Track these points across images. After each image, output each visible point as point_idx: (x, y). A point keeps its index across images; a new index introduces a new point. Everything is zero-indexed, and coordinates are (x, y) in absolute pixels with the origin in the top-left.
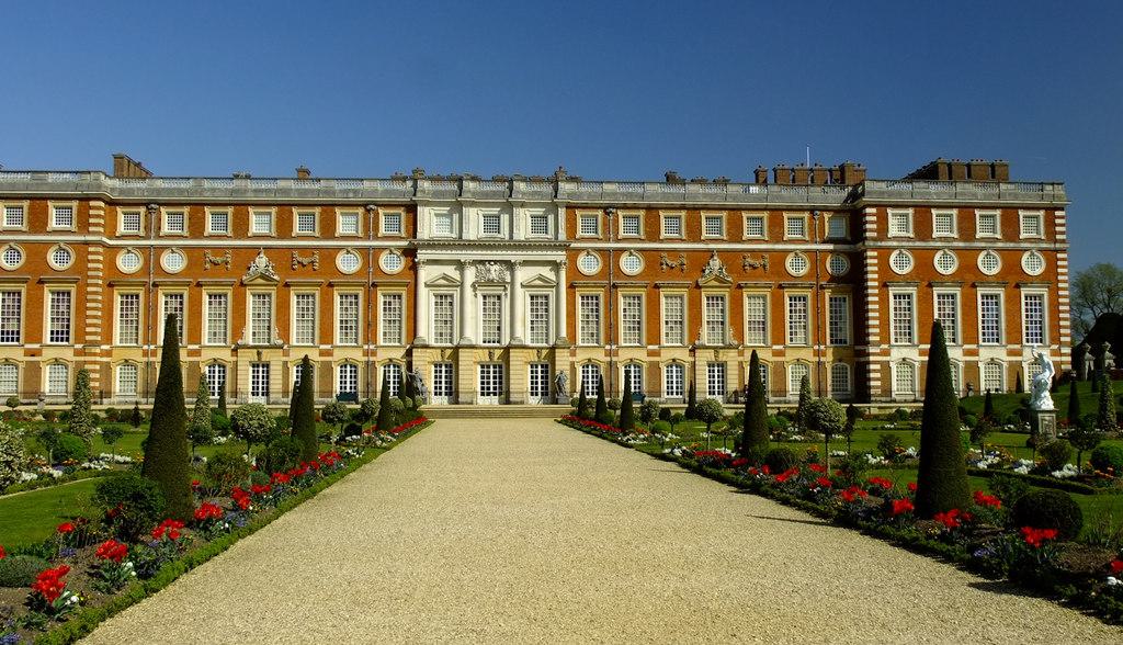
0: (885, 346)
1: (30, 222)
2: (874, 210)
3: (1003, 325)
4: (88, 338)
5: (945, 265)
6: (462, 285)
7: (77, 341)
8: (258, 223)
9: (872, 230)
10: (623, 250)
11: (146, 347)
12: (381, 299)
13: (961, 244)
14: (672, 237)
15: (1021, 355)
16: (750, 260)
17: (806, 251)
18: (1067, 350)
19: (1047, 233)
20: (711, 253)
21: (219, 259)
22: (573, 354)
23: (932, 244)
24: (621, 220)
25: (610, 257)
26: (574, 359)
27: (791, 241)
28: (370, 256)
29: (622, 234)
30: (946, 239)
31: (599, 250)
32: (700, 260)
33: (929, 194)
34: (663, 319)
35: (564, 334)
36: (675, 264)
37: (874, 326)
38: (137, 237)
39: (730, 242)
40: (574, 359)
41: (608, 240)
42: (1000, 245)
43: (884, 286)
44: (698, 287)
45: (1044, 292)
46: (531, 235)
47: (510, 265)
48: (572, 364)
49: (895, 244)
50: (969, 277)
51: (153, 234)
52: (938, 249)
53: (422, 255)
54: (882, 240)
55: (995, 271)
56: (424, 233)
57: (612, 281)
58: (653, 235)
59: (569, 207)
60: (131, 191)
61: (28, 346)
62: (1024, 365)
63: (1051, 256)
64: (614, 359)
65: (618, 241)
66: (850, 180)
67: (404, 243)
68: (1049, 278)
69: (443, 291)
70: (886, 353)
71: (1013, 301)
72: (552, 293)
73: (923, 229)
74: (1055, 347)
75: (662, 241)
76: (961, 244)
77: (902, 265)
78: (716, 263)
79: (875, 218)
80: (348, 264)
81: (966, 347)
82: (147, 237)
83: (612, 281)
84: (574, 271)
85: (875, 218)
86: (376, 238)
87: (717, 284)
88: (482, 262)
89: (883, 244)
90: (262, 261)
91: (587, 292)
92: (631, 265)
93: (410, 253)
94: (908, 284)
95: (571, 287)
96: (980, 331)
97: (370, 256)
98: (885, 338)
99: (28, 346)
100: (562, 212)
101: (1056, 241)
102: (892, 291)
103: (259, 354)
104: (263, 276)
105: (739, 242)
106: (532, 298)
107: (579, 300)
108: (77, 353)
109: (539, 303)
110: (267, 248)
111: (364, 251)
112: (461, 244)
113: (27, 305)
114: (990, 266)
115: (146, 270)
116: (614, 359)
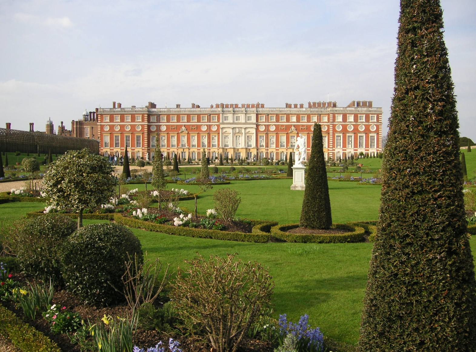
2: (332, 115)
10: (270, 125)
13: (354, 123)
14: (283, 122)
20: (292, 125)
25: (267, 127)
28: (209, 127)
29: (270, 121)
30: (351, 122)
32: (288, 127)
39: (297, 122)
41: (266, 122)
42: (364, 123)
45: (375, 135)
49: (337, 123)
50: (356, 131)
52: (348, 125)
53: (222, 126)
55: (363, 130)
57: (267, 131)
59: (257, 115)
63: (378, 127)
69: (226, 135)
70: (334, 150)
71: (367, 138)
73: (345, 119)
76: (354, 123)
78: (293, 128)
80: (204, 128)
83: (267, 131)
88: (236, 128)
89: (334, 123)
91: (261, 135)
93: (218, 126)
98: (334, 146)
102: (336, 135)
104: (183, 132)
105: (299, 122)
108: (143, 150)
109: (248, 138)
110: (185, 126)
111: (207, 125)
114: (362, 128)
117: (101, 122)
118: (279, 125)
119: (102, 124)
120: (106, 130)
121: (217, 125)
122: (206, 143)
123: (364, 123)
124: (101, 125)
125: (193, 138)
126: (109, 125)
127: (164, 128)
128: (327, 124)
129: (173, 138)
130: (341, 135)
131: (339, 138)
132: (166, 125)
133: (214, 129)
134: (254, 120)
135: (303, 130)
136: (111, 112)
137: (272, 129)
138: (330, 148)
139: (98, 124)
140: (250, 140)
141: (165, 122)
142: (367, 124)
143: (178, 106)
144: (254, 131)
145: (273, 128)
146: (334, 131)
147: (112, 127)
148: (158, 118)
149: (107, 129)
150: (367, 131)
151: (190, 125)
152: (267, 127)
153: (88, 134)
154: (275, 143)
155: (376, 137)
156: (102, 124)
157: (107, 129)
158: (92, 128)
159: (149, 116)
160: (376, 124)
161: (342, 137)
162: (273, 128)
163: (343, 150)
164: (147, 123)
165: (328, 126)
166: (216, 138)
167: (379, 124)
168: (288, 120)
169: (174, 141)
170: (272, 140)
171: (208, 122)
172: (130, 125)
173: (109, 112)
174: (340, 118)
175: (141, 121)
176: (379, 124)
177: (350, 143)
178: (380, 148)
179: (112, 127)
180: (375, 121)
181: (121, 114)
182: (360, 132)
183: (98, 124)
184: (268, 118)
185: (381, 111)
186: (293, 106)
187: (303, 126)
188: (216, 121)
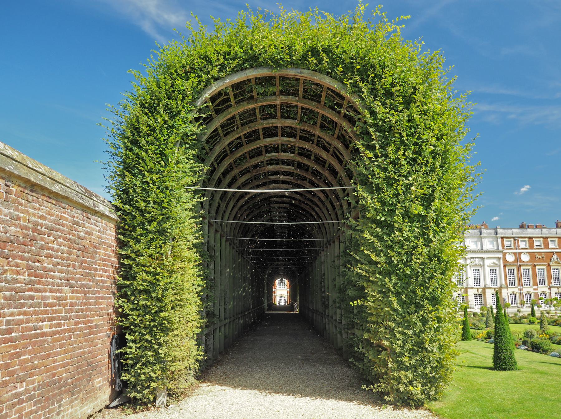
6: (500, 266)
44: (549, 265)
47: (483, 258)
65: (520, 249)
72: (497, 268)
84: (505, 261)
92: (525, 258)
95: (505, 266)
100: (500, 240)
107: (507, 271)
109: (493, 271)
112: (482, 251)
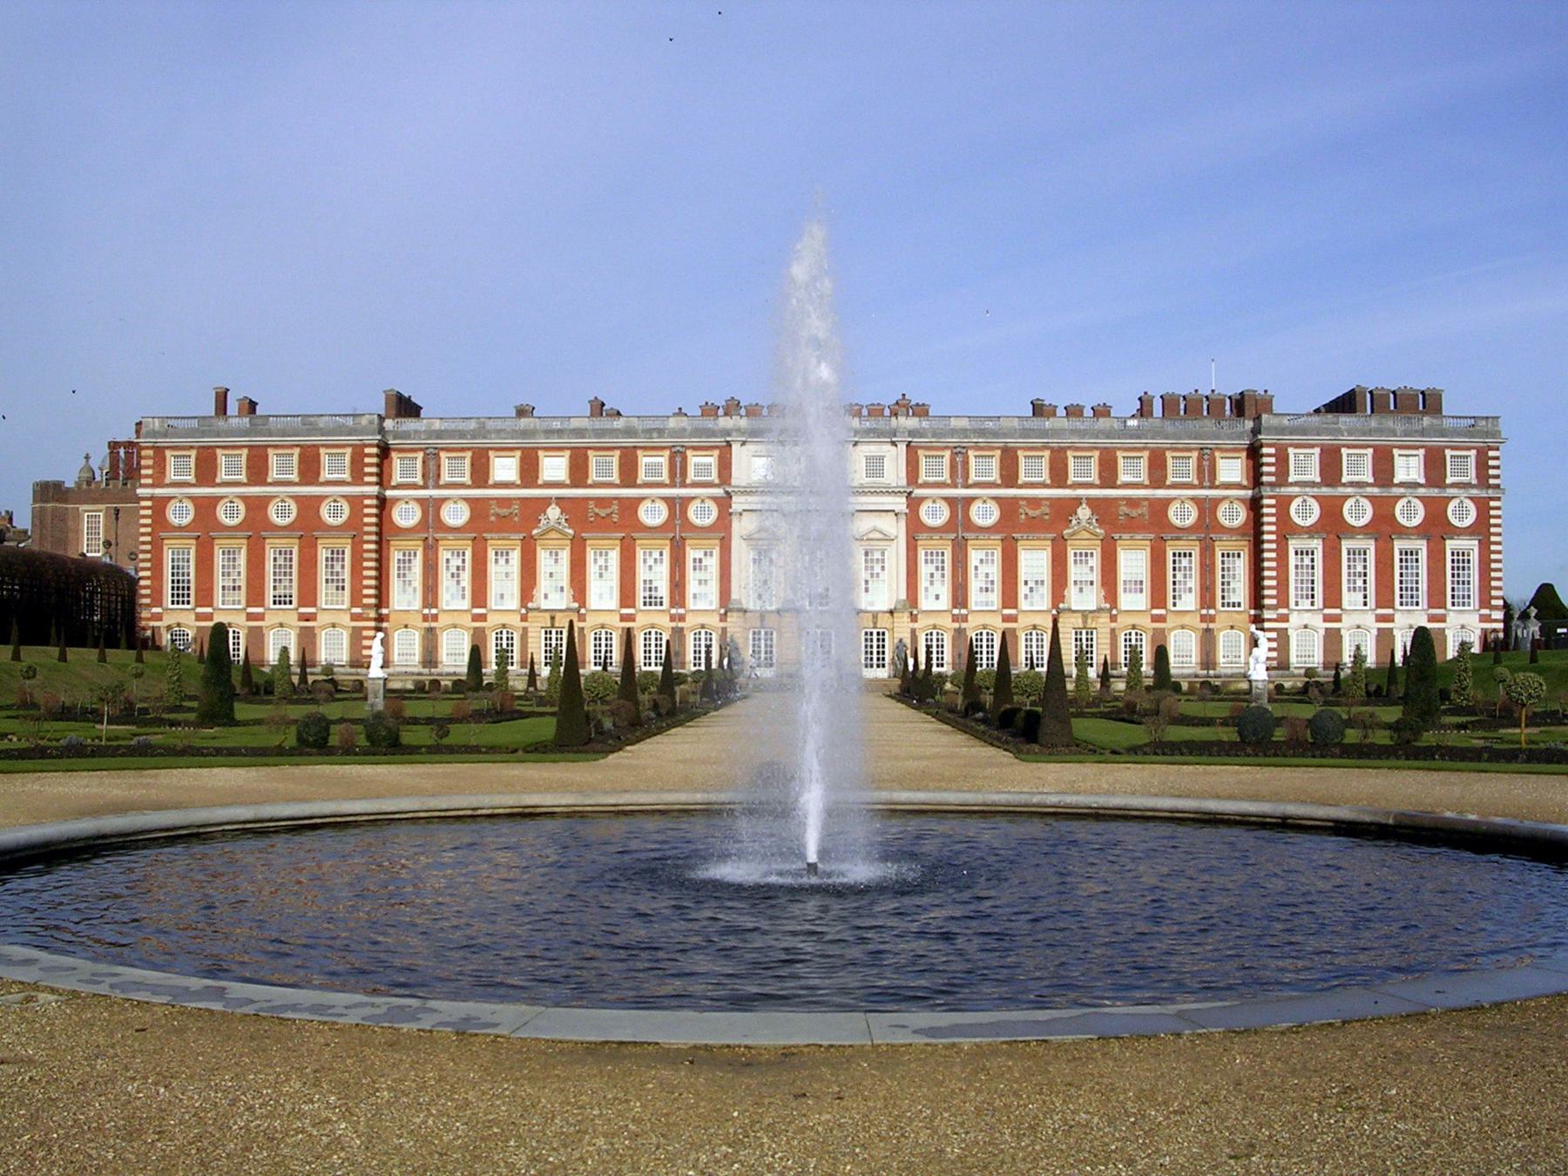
0: (1284, 611)
1: (301, 473)
3: (1423, 586)
4: (366, 601)
5: (1358, 513)
7: (353, 604)
8: (554, 467)
9: (1269, 474)
11: (426, 611)
12: (692, 554)
13: (1376, 491)
15: (1444, 621)
16: (1124, 509)
17: (1193, 499)
18: (1499, 615)
19: (1478, 477)
20: (1078, 501)
21: (504, 512)
22: (914, 618)
23: (1341, 491)
24: (972, 460)
25: (960, 507)
26: (915, 625)
27: (1175, 486)
29: (973, 478)
31: (946, 499)
32: (1064, 510)
33: (1340, 432)
34: (1022, 577)
35: (903, 596)
36: (1031, 513)
37: (1270, 587)
38: (414, 486)
39: (1101, 487)
40: (915, 625)
41: (955, 486)
42: (1422, 491)
43: (1282, 541)
45: (1471, 545)
46: (866, 481)
48: (913, 631)
50: (1384, 527)
51: (431, 483)
53: (738, 503)
54: (1281, 486)
55: (1416, 521)
56: (739, 476)
57: (960, 528)
58: (1009, 476)
60: (406, 435)
61: (302, 610)
62: (1447, 632)
63: (1483, 506)
64: (964, 625)
66: (1250, 410)
67: (719, 492)
68: (1481, 529)
70: (1285, 618)
71: (1436, 557)
74: (1485, 611)
75: (1021, 487)
76: (1376, 491)
77: (1305, 512)
78: (1084, 512)
79: (1273, 460)
80: (653, 514)
81: (1380, 611)
82: (425, 487)
83: (960, 528)
85: (1273, 460)
86: (684, 485)
87: (1087, 535)
89: (1285, 491)
90: (554, 512)
93: (724, 503)
94: (1312, 537)
96: (1397, 592)
97: (678, 507)
98: (1283, 601)
99: (302, 610)
101: (1489, 486)
102: (1293, 544)
103: (553, 618)
105: (1114, 486)
106: (866, 554)
110: (560, 500)
113: (300, 565)
115: (423, 525)
116: (964, 625)
117: (152, 486)
118: (1015, 499)
119: (159, 491)
120: (175, 521)
121: (715, 499)
122: (664, 590)
123: (1422, 491)
124: (151, 498)
125: (601, 561)
126: (192, 498)
127: (454, 514)
128: (1242, 493)
129: (502, 561)
130: (1316, 544)
131: (1307, 561)
132: (466, 499)
133: (702, 515)
134: (894, 472)
135: (1132, 526)
136: (204, 434)
137: (984, 517)
138: (1271, 607)
139: (139, 491)
140: (877, 569)
141: (462, 486)
142: (1434, 492)
143: (522, 412)
144: (898, 529)
145: (984, 514)
146: (1287, 529)
147: (205, 507)
148: (432, 464)
149: (180, 514)
150: (1436, 528)
151: (586, 499)
152: (960, 507)
153: (90, 538)
154: (997, 587)
155: (1475, 557)
156: (159, 491)
157: (180, 514)
158: (117, 511)
159: (385, 452)
160: (1474, 492)
161: (1319, 556)
162: (984, 514)
163: (1327, 619)
164: (375, 490)
165: (1255, 505)
166: (713, 563)
167: (1491, 493)
168: (1059, 476)
169: (504, 576)
170: (983, 569)
171: (673, 485)
172: (296, 498)
173: (190, 433)
174: (1305, 465)
175: (346, 476)
176: (1491, 493)
177: (1360, 583)
178: (1496, 608)
179: (205, 507)
180: (1472, 477)
181: (250, 447)
182: (1404, 532)
183: (139, 491)
184: (966, 463)
185: (1496, 434)
186: (1088, 412)
187: (1133, 502)
188: (714, 477)
